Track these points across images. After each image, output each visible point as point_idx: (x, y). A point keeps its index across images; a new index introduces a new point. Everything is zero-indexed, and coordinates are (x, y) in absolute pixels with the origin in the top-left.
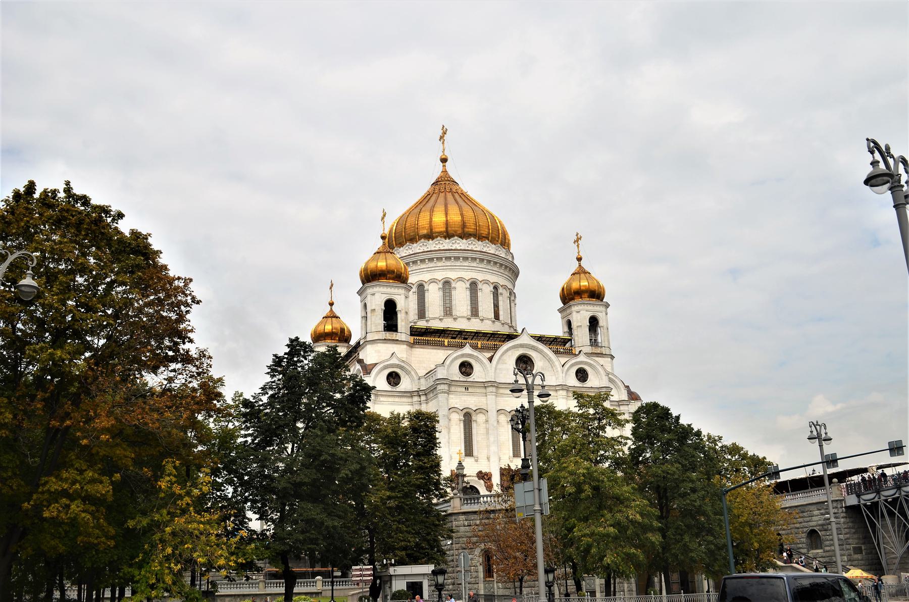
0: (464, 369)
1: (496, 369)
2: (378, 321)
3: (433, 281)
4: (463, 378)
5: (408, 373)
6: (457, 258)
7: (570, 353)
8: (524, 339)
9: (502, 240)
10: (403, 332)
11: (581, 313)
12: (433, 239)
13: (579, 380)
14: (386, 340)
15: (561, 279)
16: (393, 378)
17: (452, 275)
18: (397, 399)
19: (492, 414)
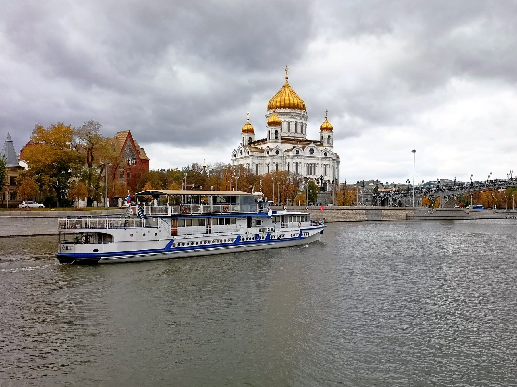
2: (273, 136)
3: (285, 121)
8: (312, 144)
14: (275, 142)
16: (277, 152)
19: (303, 164)
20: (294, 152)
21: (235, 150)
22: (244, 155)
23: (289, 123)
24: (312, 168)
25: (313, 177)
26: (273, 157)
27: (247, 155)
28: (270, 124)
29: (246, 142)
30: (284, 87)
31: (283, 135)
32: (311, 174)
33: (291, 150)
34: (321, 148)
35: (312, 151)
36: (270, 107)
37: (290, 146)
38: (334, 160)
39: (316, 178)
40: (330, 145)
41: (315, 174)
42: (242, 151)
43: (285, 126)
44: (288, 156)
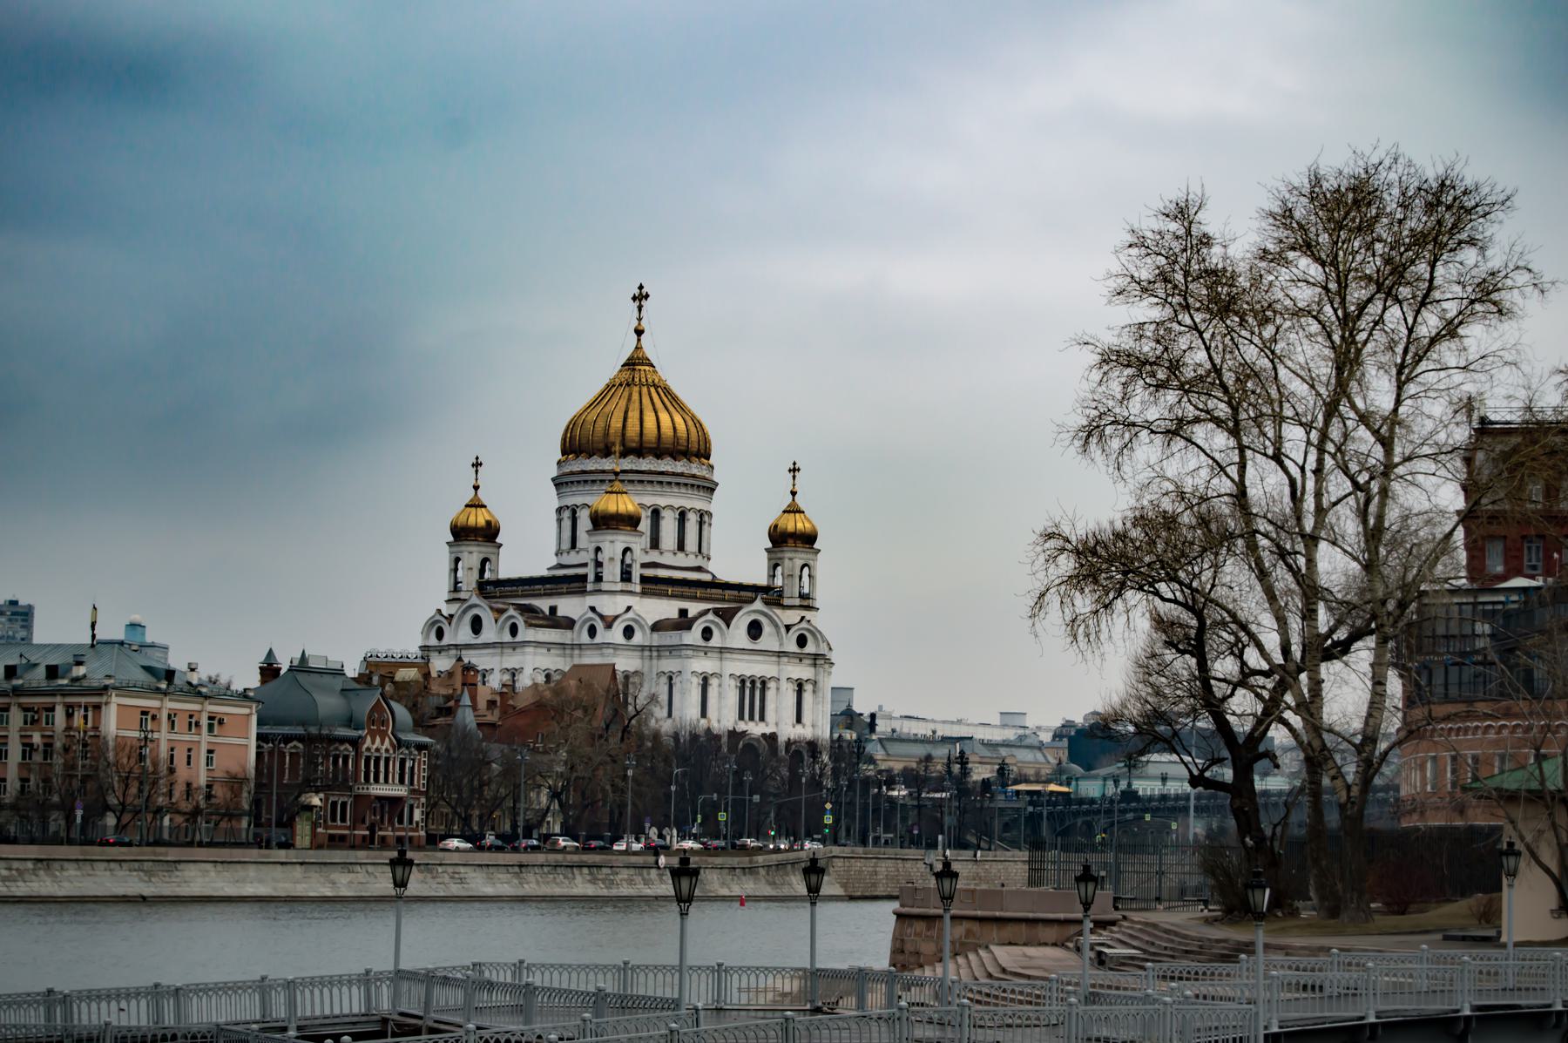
2: (612, 572)
4: (703, 643)
8: (758, 605)
15: (770, 512)
16: (629, 632)
22: (489, 633)
23: (656, 514)
24: (753, 692)
25: (756, 729)
27: (507, 637)
29: (469, 579)
32: (752, 718)
35: (755, 630)
37: (667, 609)
39: (768, 731)
40: (806, 602)
41: (762, 718)
43: (645, 526)
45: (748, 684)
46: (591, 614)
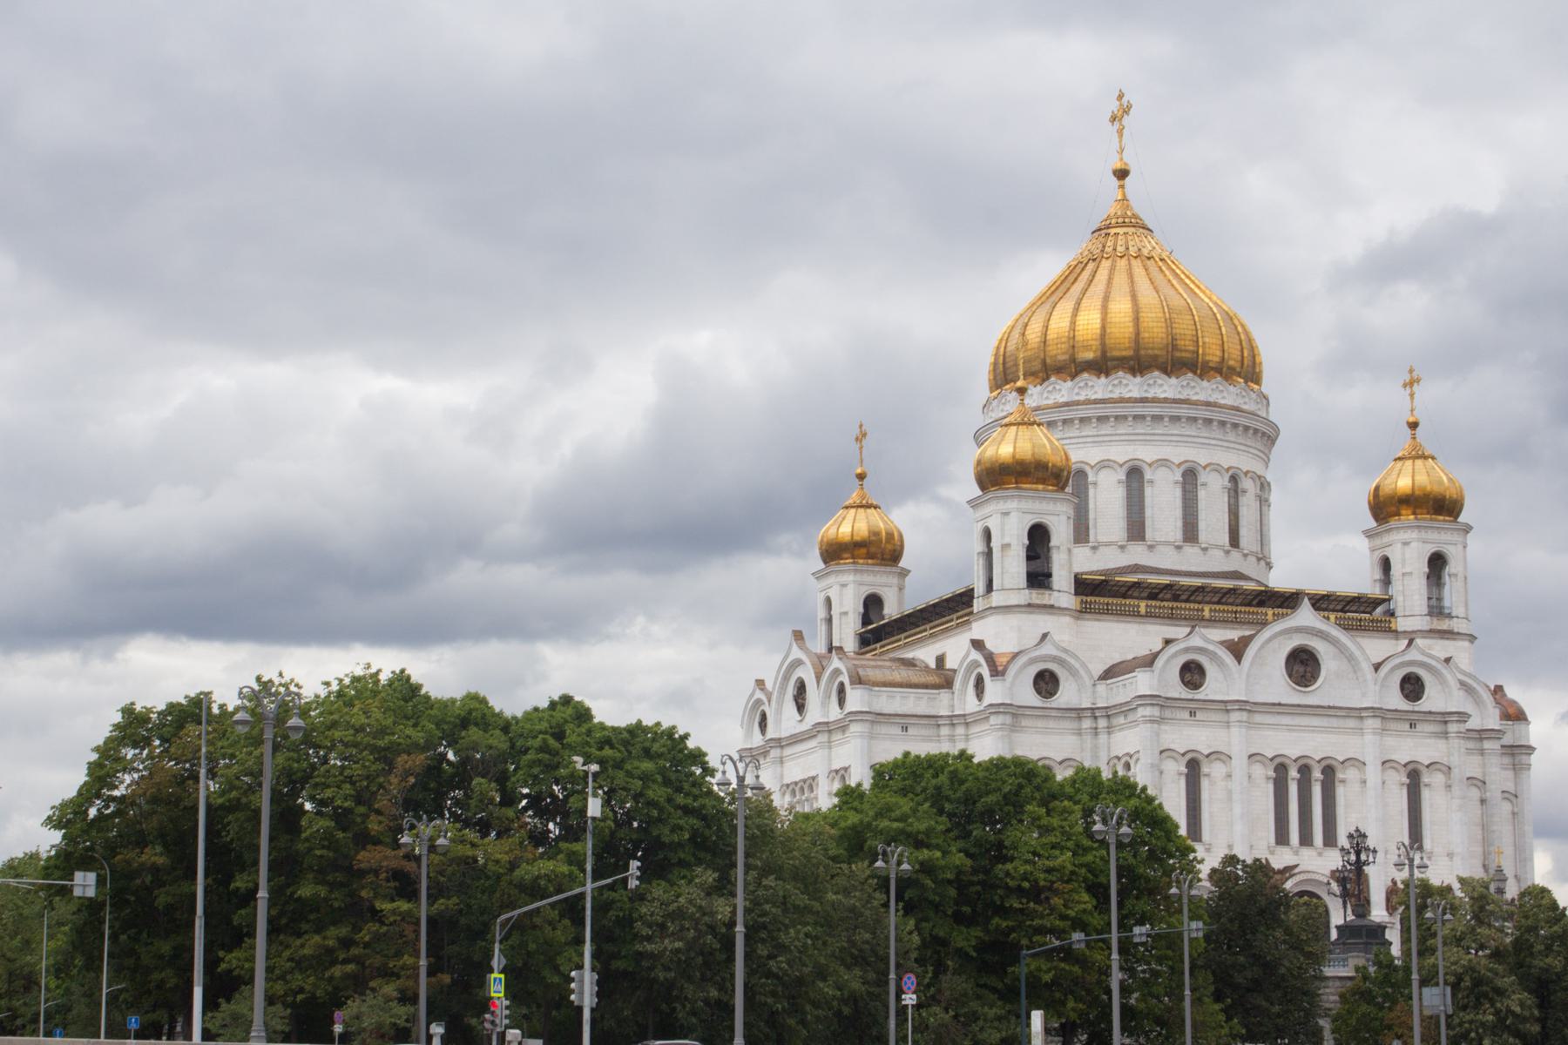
0: (1188, 677)
1: (1248, 676)
2: (1011, 567)
3: (1104, 464)
4: (1185, 693)
5: (1073, 672)
6: (1157, 418)
7: (1385, 627)
8: (1305, 615)
9: (1247, 371)
10: (1062, 591)
11: (1410, 547)
12: (1107, 375)
13: (1407, 697)
14: (1031, 607)
16: (1046, 682)
17: (1146, 453)
18: (1052, 724)
20: (1164, 680)
21: (760, 683)
22: (814, 714)
24: (1304, 790)
26: (1014, 713)
27: (835, 713)
28: (997, 477)
29: (847, 631)
30: (1103, 230)
31: (1088, 562)
33: (1149, 661)
34: (1376, 647)
35: (1303, 665)
36: (1004, 375)
38: (1482, 735)
42: (801, 688)
44: (1126, 709)
45: (1293, 773)
46: (976, 655)
